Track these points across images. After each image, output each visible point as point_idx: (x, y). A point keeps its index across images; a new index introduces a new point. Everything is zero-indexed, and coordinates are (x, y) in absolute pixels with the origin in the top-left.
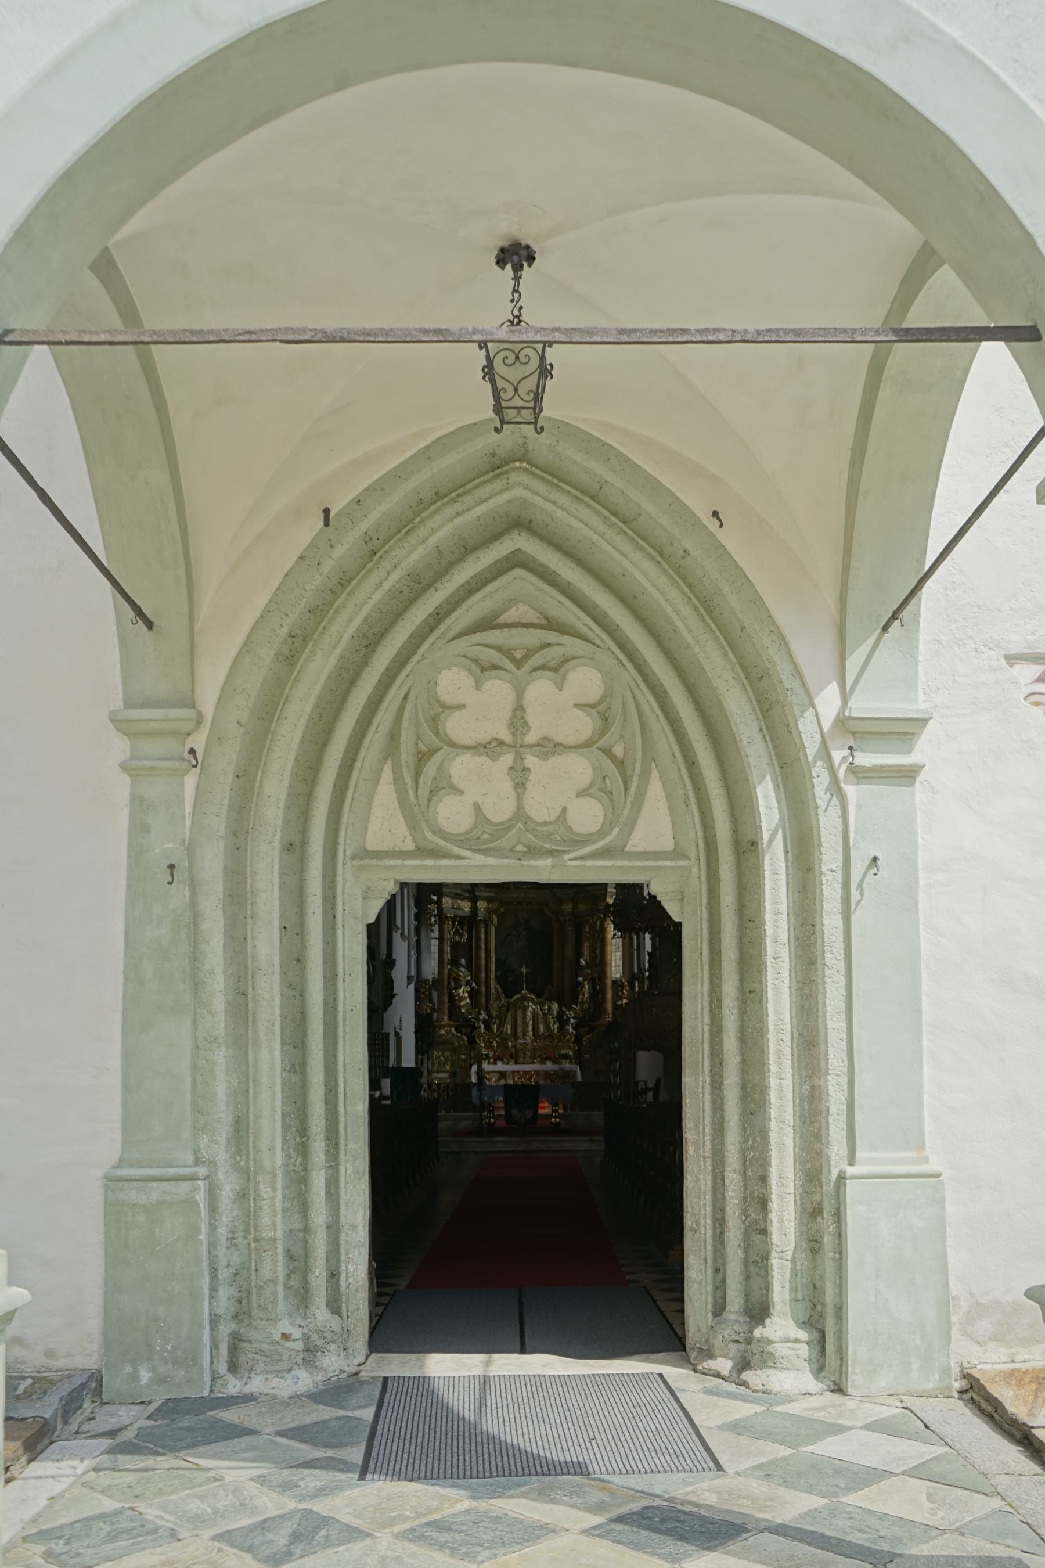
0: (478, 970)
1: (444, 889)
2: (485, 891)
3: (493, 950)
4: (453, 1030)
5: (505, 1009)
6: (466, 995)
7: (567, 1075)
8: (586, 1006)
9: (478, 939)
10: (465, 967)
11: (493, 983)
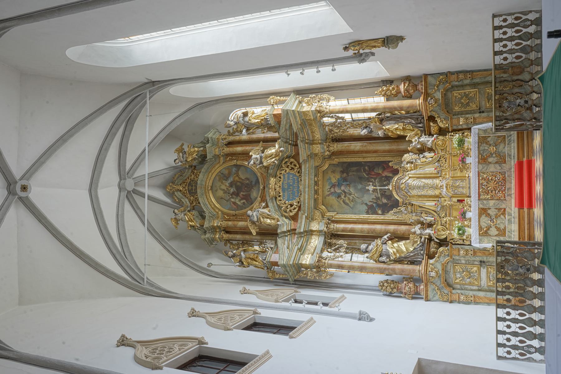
0: (374, 231)
2: (301, 222)
3: (357, 217)
4: (431, 261)
5: (409, 207)
6: (395, 245)
7: (482, 140)
8: (410, 127)
10: (370, 244)
11: (390, 216)
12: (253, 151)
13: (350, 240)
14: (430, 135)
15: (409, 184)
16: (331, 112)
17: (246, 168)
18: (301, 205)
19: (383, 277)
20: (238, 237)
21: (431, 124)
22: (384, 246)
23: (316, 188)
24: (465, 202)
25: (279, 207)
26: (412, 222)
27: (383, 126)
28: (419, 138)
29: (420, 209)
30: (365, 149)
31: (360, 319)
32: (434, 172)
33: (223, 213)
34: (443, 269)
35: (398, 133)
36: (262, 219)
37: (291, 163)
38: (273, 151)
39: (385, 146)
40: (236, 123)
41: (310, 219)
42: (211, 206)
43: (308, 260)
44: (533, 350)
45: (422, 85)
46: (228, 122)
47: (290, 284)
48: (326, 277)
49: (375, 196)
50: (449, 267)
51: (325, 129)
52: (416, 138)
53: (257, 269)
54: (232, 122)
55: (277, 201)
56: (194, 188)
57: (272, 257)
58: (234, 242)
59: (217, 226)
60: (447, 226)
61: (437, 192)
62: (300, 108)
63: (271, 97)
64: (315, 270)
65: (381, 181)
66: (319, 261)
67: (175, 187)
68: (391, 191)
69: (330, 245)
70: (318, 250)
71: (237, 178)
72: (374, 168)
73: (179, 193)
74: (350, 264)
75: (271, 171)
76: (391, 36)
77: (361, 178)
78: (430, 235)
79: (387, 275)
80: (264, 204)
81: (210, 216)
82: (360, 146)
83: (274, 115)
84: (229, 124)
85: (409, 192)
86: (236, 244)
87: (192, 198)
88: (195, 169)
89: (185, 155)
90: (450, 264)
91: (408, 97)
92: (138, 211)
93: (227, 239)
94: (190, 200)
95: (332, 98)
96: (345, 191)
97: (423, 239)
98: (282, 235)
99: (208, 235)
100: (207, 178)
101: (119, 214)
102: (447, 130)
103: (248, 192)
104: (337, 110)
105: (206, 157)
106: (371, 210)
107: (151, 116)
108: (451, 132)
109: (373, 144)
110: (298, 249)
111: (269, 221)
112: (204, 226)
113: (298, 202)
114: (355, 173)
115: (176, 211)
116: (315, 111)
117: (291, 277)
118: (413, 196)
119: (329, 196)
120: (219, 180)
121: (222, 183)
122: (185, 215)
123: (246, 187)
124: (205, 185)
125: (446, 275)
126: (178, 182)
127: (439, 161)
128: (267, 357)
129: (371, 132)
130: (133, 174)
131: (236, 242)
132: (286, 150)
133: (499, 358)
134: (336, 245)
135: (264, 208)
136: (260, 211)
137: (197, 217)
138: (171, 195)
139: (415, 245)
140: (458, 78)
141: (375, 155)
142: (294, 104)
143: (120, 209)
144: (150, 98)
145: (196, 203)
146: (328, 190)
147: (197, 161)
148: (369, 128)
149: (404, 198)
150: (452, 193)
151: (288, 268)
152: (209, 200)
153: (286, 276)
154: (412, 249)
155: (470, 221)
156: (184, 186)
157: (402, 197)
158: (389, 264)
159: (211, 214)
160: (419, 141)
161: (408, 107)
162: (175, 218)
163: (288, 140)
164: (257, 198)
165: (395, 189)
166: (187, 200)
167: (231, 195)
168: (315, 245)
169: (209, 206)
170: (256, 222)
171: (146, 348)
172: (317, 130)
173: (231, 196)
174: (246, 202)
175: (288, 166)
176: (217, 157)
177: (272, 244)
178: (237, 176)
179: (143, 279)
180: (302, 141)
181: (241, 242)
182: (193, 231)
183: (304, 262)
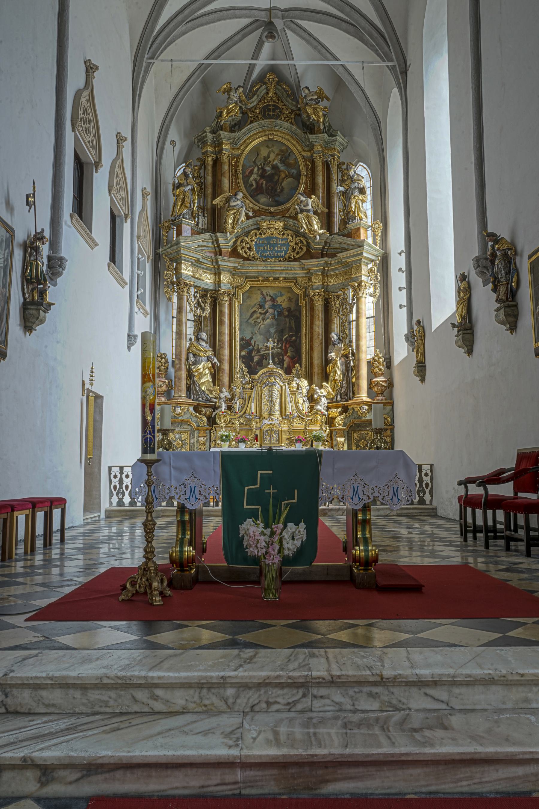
0: (222, 347)
1: (182, 252)
2: (229, 261)
4: (191, 409)
5: (249, 386)
6: (207, 371)
9: (221, 312)
10: (206, 343)
11: (238, 365)
12: (316, 199)
13: (210, 320)
14: (328, 408)
15: (274, 387)
16: (358, 299)
17: (296, 188)
18: (250, 260)
19: (170, 358)
20: (209, 179)
21: (340, 410)
22: (206, 358)
23: (271, 278)
24: (255, 442)
25: (247, 234)
26: (233, 388)
27: (340, 358)
28: (325, 396)
29: (247, 397)
30: (315, 337)
31: (129, 336)
32: (287, 411)
33: (239, 156)
34: (183, 420)
35: (332, 374)
36: (232, 212)
37: (301, 248)
38: (316, 227)
39: (317, 361)
40: (352, 178)
41: (234, 273)
42: (248, 138)
43: (186, 272)
44: (120, 496)
45: (382, 400)
46: (353, 167)
47: (156, 249)
48: (167, 293)
49: (261, 348)
50: (185, 427)
51: (340, 290)
52: (325, 394)
53: (171, 206)
54: (353, 173)
55: (255, 231)
56: (271, 113)
57: (188, 227)
58: (202, 171)
59: (222, 149)
60: (229, 425)
61: (265, 414)
62: (366, 261)
63: (381, 225)
64: (175, 279)
65: (278, 355)
66: (185, 284)
67: (273, 85)
68: (266, 367)
69: (204, 296)
70: (198, 283)
71: (283, 175)
72: (293, 348)
73: (265, 91)
74: (184, 320)
75: (292, 223)
76: (425, 370)
77: (281, 332)
78: (220, 407)
79: (173, 362)
80: (251, 214)
81: (234, 138)
82: (318, 332)
83: (359, 229)
84: (351, 168)
85: (266, 386)
86: (200, 174)
87: (258, 111)
88: (296, 115)
89: (314, 103)
90: (189, 428)
91: (370, 385)
92: (239, 36)
93: (206, 163)
94: (255, 107)
95: (375, 300)
96: (268, 314)
97: (214, 400)
98: (214, 238)
99: (210, 136)
100: (283, 133)
101: (236, 11)
102: (333, 425)
103: (266, 191)
104: (360, 306)
105: (311, 133)
106: (246, 344)
107: (363, 68)
108: (330, 430)
109: (320, 346)
110: (198, 259)
111: (230, 221)
112: (221, 132)
113: (253, 257)
114: (288, 325)
115: (241, 90)
116: (360, 280)
117: (165, 250)
118: (261, 390)
119: (261, 294)
120: (281, 151)
121: (278, 155)
122: (236, 103)
123: (272, 188)
124: (275, 131)
125: (177, 424)
126: (279, 90)
127: (299, 417)
128: (92, 244)
129: (334, 345)
130: (289, 28)
131: (202, 175)
132: (316, 243)
133: (110, 468)
134: (203, 303)
135: (246, 214)
136: (242, 210)
137: (233, 120)
138: (262, 79)
139: (207, 392)
140: (386, 436)
141: (308, 347)
142: (370, 254)
143: (243, 12)
144: (387, 66)
145: (251, 117)
146: (268, 294)
147: (306, 118)
148: (339, 343)
149: (259, 381)
150: (265, 430)
151: (175, 247)
152: (255, 137)
153: (165, 244)
154: (203, 388)
155: (235, 447)
156: (274, 99)
157: (261, 378)
158: (185, 364)
159: (237, 140)
160: (321, 396)
161: (358, 386)
162: (230, 89)
163: (328, 245)
164: (259, 203)
165: (269, 371)
166: (255, 103)
167: (262, 168)
168: (203, 279)
169: (248, 136)
170: (229, 205)
171: (87, 100)
172: (340, 282)
173: (260, 167)
174: (253, 188)
175: (298, 245)
176: (311, 147)
177: (202, 224)
178: (286, 176)
179: (152, 58)
180: (326, 263)
181: (203, 181)
182: (215, 114)
183: (183, 266)
